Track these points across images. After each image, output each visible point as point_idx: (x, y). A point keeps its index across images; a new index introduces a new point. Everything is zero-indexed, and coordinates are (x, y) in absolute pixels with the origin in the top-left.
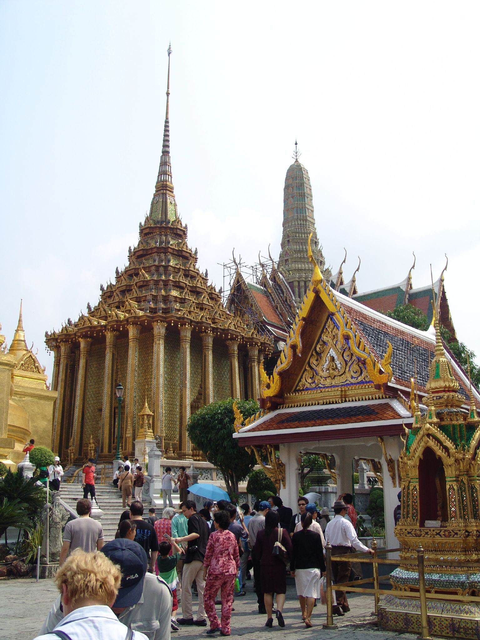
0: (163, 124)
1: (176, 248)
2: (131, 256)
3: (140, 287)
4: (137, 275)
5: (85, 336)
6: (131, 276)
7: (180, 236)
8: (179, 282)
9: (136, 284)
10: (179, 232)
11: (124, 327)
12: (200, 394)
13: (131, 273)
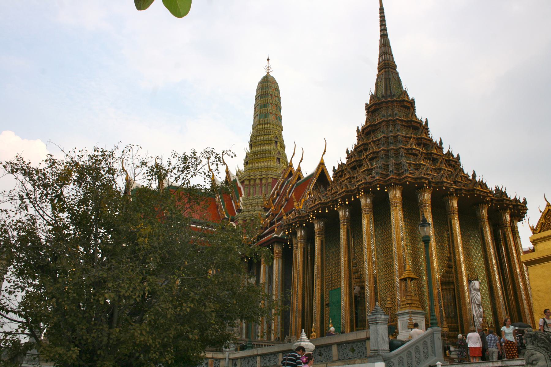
0: (378, 11)
2: (360, 135)
3: (371, 160)
4: (366, 150)
5: (319, 217)
6: (361, 151)
7: (408, 108)
8: (412, 149)
9: (367, 158)
11: (355, 198)
12: (450, 267)
13: (359, 149)
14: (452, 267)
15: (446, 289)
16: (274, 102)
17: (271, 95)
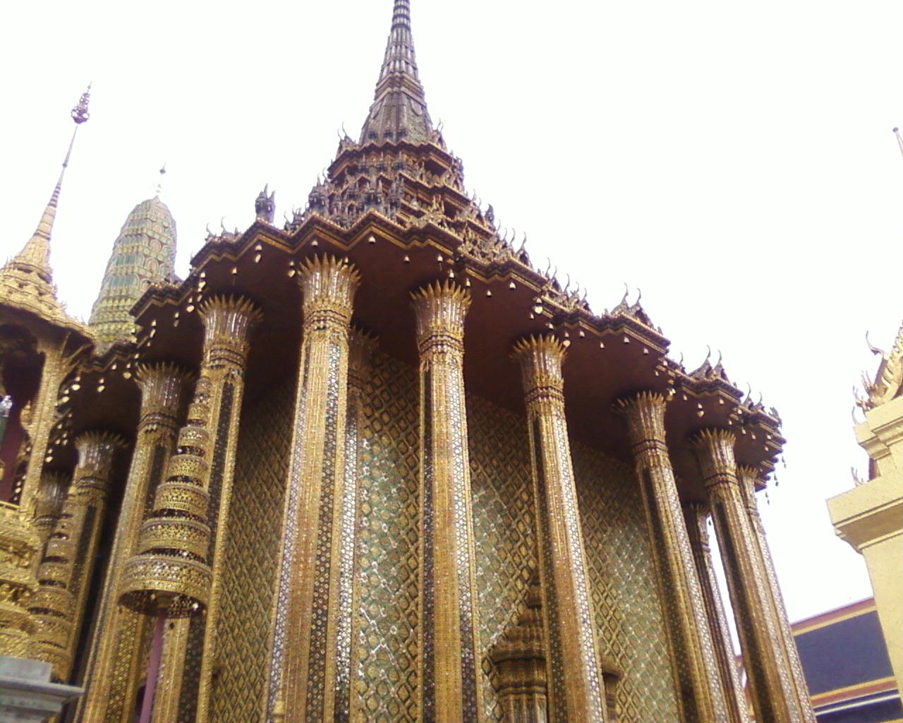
1: (424, 183)
10: (433, 158)
14: (539, 607)
15: (516, 685)
16: (153, 255)
17: (150, 238)
